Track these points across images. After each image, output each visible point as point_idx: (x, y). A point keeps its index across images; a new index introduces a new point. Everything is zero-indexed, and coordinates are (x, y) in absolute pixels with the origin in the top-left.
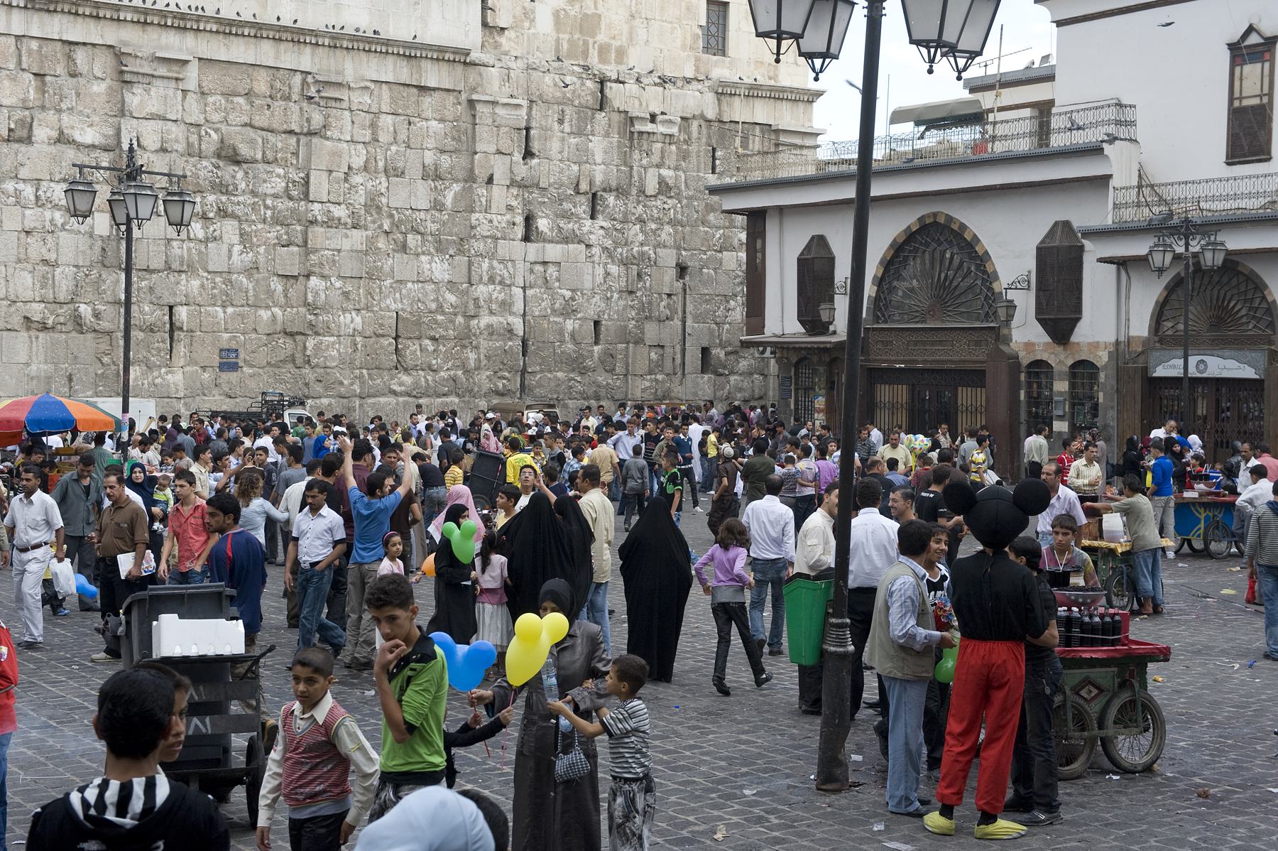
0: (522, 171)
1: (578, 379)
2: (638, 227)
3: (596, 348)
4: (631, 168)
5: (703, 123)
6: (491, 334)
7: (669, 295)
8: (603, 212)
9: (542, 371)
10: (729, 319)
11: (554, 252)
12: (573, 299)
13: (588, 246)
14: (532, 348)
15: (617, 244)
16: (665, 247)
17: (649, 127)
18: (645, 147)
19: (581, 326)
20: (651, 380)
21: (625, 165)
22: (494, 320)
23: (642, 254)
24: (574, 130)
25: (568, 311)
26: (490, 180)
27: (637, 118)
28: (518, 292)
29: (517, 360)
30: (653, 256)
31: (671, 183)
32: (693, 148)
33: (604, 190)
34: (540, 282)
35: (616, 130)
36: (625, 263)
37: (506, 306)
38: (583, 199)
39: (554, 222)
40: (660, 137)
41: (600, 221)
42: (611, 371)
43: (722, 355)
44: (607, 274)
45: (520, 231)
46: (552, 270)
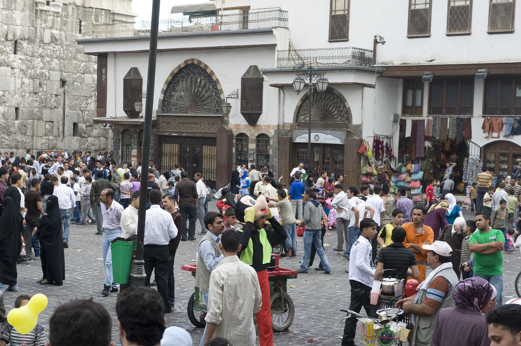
1: (7, 138)
2: (40, 59)
3: (17, 122)
4: (36, 28)
5: (75, 7)
7: (56, 95)
8: (21, 51)
10: (88, 109)
12: (4, 96)
13: (12, 68)
15: (28, 68)
16: (54, 70)
17: (46, 8)
18: (44, 18)
19: (8, 110)
20: (46, 139)
21: (33, 26)
23: (42, 74)
24: (5, 7)
27: (39, 2)
30: (47, 74)
31: (58, 37)
32: (70, 20)
33: (21, 39)
35: (28, 8)
36: (32, 78)
38: (10, 43)
40: (52, 13)
41: (19, 55)
42: (25, 134)
43: (84, 127)
44: (23, 83)
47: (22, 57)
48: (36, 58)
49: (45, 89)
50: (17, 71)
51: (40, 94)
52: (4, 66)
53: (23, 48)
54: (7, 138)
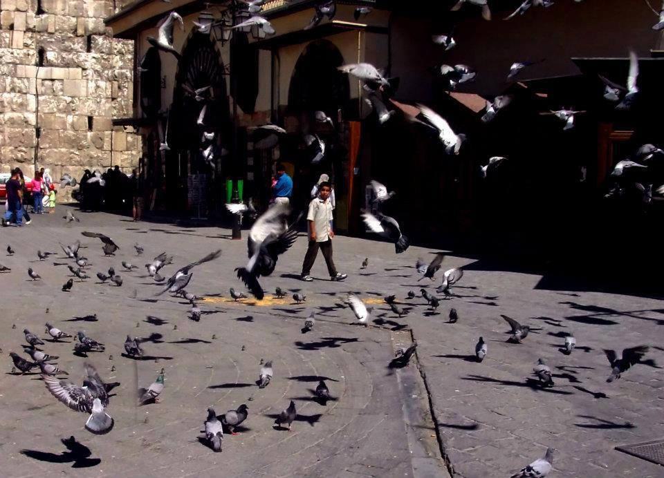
0: (34, 21)
1: (77, 153)
2: (118, 57)
3: (90, 134)
6: (12, 124)
8: (95, 47)
9: (50, 147)
11: (58, 73)
12: (72, 102)
13: (84, 69)
14: (43, 132)
15: (104, 68)
19: (78, 119)
20: (128, 155)
22: (15, 115)
23: (122, 74)
25: (69, 110)
26: (12, 27)
28: (32, 100)
29: (32, 140)
34: (49, 91)
36: (108, 80)
37: (23, 106)
39: (59, 54)
42: (101, 148)
44: (98, 87)
45: (35, 59)
46: (57, 85)
47: (98, 55)
48: (114, 56)
49: (125, 93)
50: (90, 72)
51: (119, 99)
52: (73, 67)
53: (98, 44)
54: (77, 153)
